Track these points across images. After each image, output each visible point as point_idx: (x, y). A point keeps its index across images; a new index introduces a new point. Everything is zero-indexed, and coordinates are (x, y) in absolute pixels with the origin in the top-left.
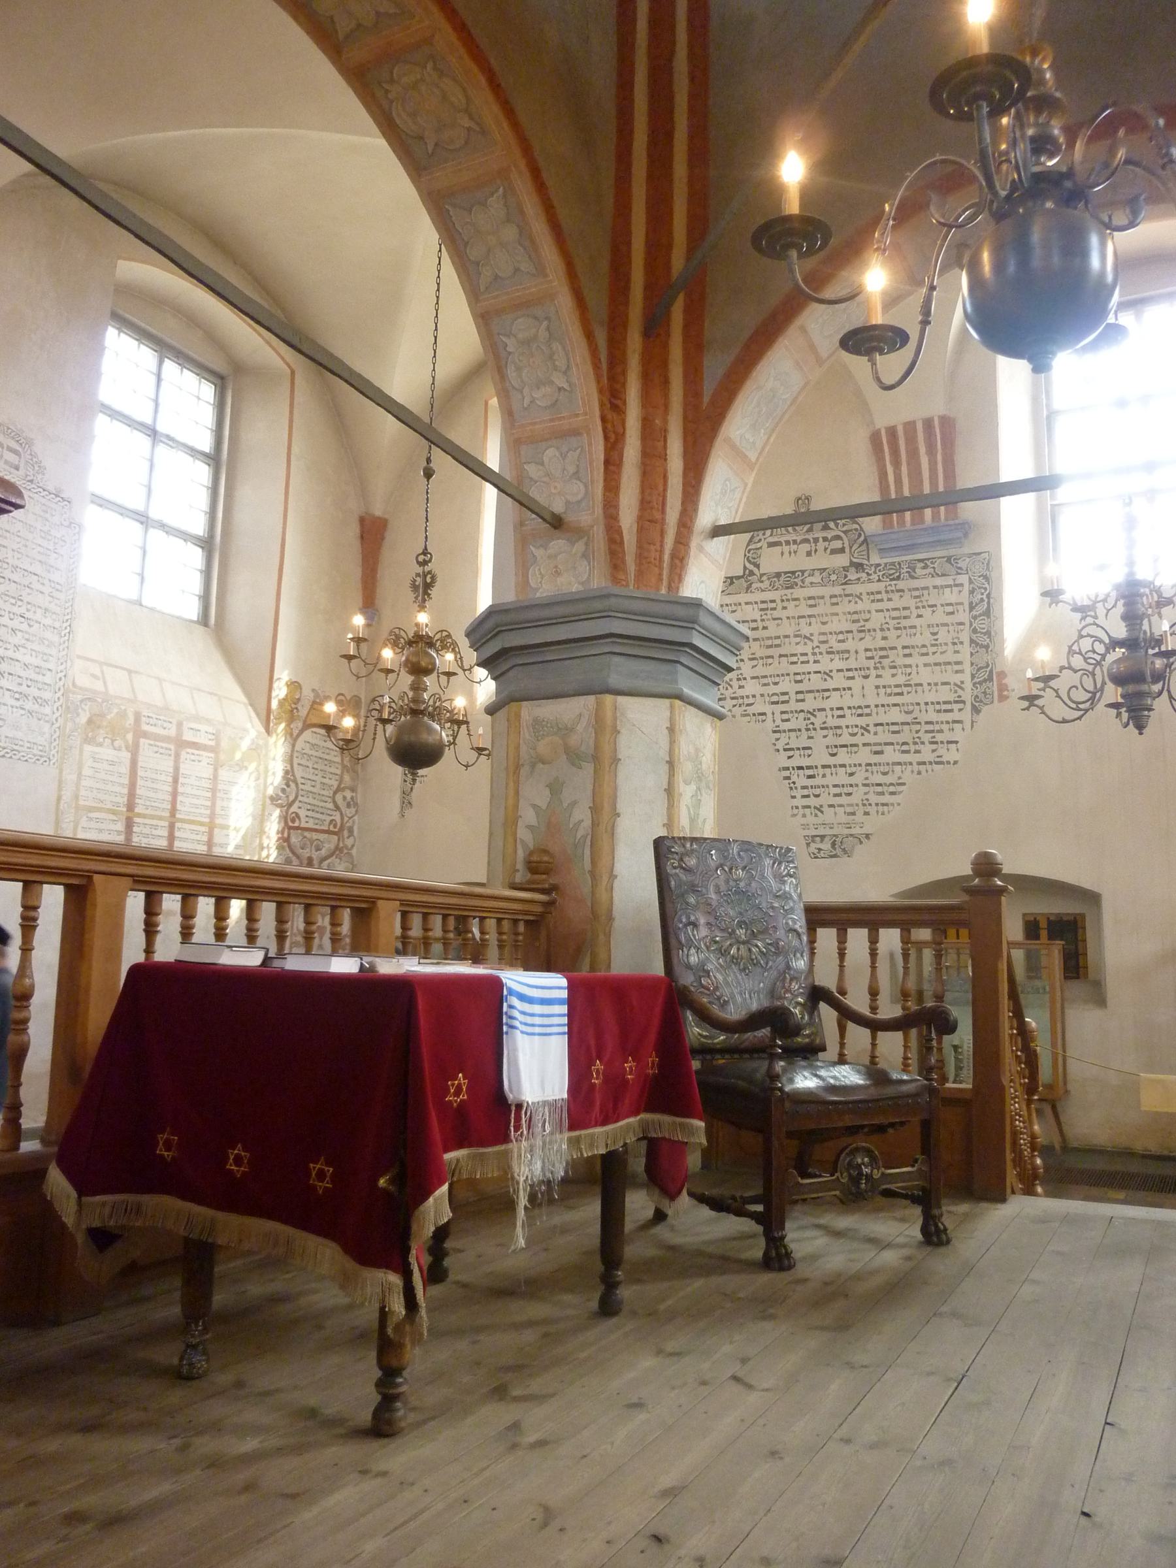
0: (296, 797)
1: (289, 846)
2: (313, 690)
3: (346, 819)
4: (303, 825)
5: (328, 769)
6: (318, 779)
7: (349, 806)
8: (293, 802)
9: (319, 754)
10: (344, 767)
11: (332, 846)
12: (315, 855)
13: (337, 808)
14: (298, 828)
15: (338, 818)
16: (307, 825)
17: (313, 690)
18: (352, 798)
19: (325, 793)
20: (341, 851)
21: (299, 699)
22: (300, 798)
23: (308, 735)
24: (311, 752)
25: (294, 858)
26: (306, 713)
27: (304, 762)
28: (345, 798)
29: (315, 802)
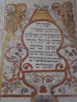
0: (27, 56)
1: (25, 82)
2: (35, 5)
3: (70, 62)
4: (35, 68)
5: (51, 39)
6: (44, 44)
7: (71, 55)
8: (25, 58)
9: (44, 33)
10: (63, 36)
11: (61, 78)
12: (47, 85)
13: (61, 57)
14: (31, 71)
15: (63, 62)
16: (37, 69)
17: (35, 5)
18: (73, 51)
19: (51, 50)
20: (69, 80)
21: (25, 11)
22: (30, 56)
23: (34, 25)
24: (36, 33)
25: (29, 88)
26: (31, 16)
27: (32, 38)
28: (67, 51)
29: (43, 56)
